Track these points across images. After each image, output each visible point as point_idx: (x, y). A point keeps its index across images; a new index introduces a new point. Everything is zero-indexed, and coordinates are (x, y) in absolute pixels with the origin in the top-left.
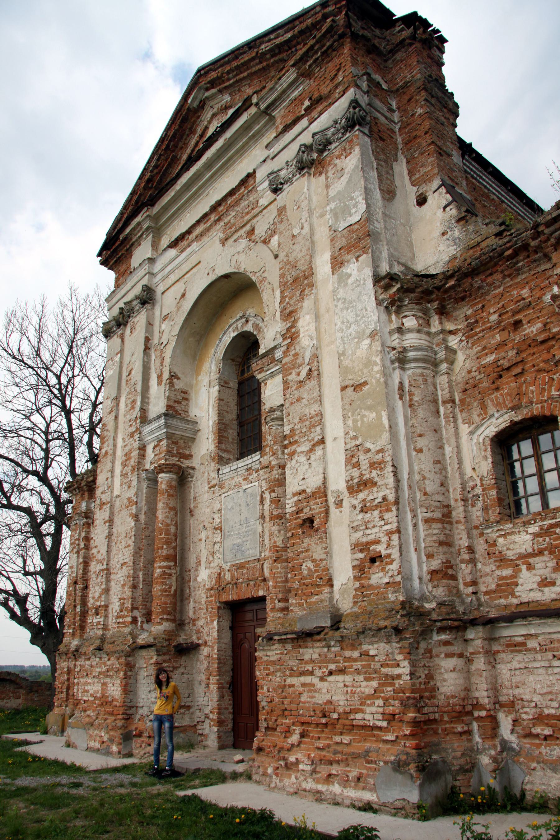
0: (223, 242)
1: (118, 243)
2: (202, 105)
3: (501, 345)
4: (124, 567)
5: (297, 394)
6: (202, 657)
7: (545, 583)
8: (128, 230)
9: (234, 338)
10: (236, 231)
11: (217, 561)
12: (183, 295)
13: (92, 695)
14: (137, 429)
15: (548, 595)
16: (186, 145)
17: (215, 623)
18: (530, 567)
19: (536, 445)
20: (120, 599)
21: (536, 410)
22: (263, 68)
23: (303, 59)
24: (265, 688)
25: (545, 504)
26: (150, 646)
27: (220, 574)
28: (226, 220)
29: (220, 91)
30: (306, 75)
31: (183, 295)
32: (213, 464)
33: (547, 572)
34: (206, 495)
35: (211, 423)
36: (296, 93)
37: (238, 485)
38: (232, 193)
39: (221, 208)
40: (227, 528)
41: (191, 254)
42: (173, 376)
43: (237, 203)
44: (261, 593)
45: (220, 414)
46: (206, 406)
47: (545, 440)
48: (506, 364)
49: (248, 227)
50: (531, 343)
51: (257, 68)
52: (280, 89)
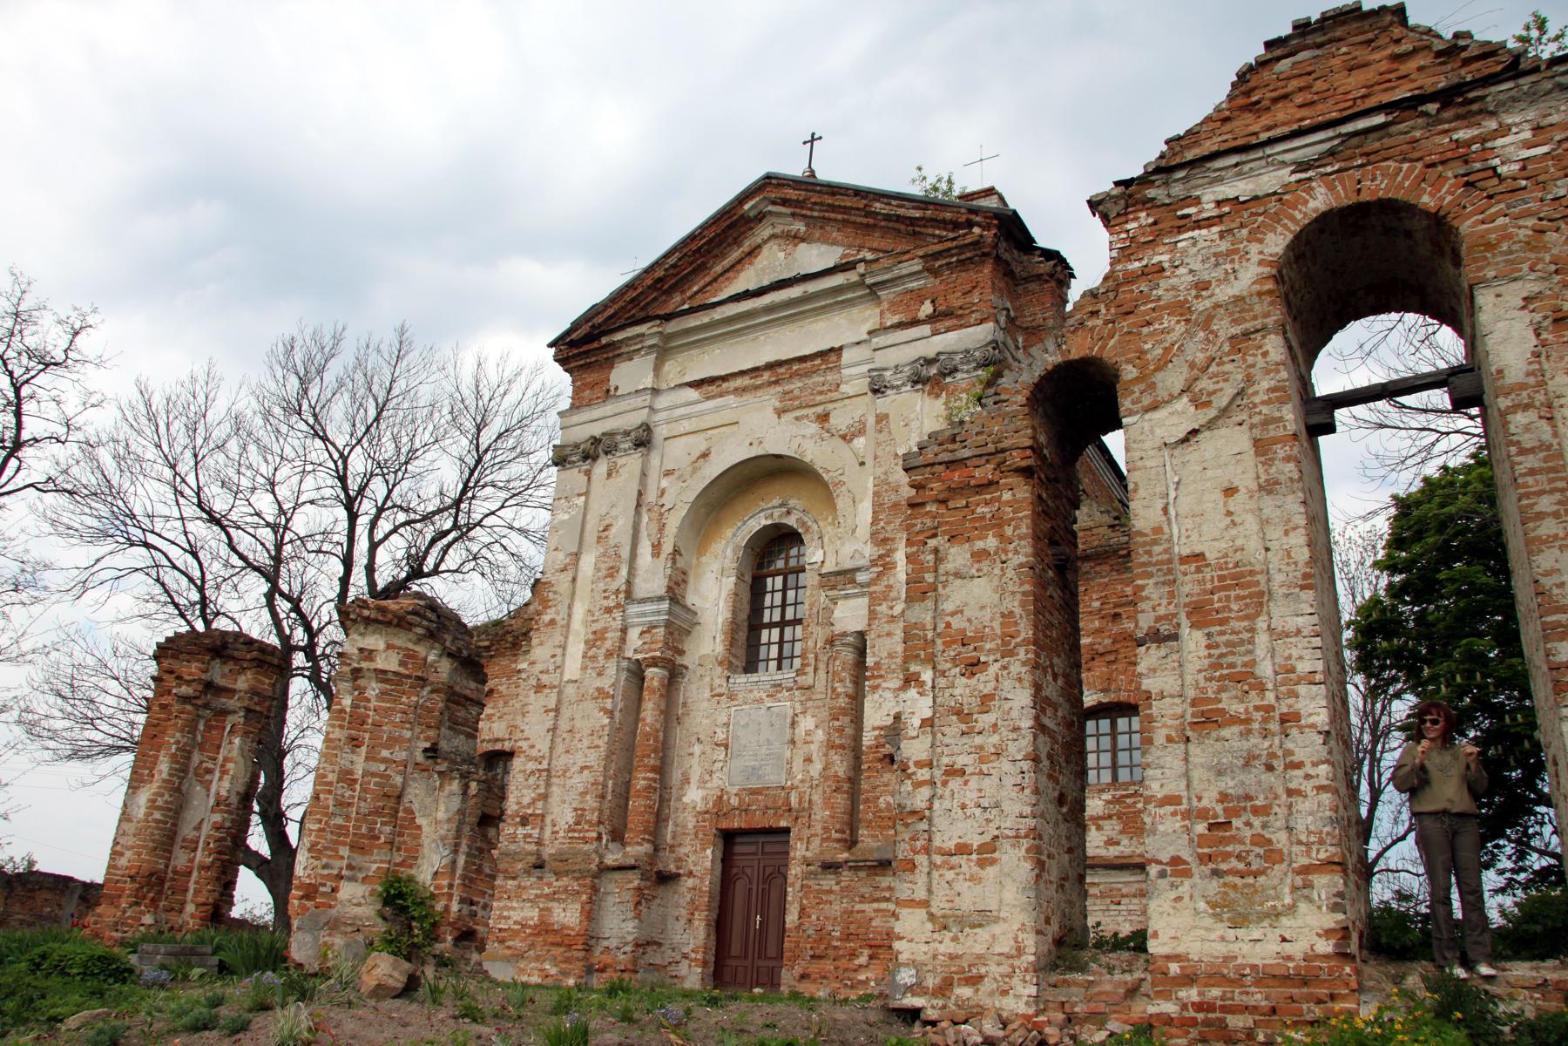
0: (780, 412)
1: (595, 345)
2: (760, 217)
3: (1099, 631)
4: (586, 772)
5: (887, 628)
6: (684, 889)
7: (1111, 842)
8: (619, 336)
9: (765, 527)
10: (801, 407)
11: (716, 782)
13: (516, 923)
14: (618, 606)
15: (1113, 851)
16: (723, 256)
17: (709, 852)
18: (1099, 828)
19: (1114, 725)
20: (576, 810)
21: (1123, 696)
22: (868, 225)
24: (814, 917)
25: (1115, 777)
26: (633, 868)
27: (720, 797)
28: (787, 388)
29: (793, 215)
30: (935, 273)
31: (705, 455)
32: (719, 669)
33: (1113, 834)
34: (705, 704)
35: (720, 620)
36: (915, 284)
37: (760, 701)
38: (802, 359)
39: (782, 370)
40: (734, 746)
41: (723, 408)
42: (676, 552)
43: (808, 374)
44: (783, 824)
45: (734, 613)
46: (715, 594)
47: (1122, 723)
48: (1101, 650)
49: (819, 409)
51: (859, 220)
52: (896, 273)
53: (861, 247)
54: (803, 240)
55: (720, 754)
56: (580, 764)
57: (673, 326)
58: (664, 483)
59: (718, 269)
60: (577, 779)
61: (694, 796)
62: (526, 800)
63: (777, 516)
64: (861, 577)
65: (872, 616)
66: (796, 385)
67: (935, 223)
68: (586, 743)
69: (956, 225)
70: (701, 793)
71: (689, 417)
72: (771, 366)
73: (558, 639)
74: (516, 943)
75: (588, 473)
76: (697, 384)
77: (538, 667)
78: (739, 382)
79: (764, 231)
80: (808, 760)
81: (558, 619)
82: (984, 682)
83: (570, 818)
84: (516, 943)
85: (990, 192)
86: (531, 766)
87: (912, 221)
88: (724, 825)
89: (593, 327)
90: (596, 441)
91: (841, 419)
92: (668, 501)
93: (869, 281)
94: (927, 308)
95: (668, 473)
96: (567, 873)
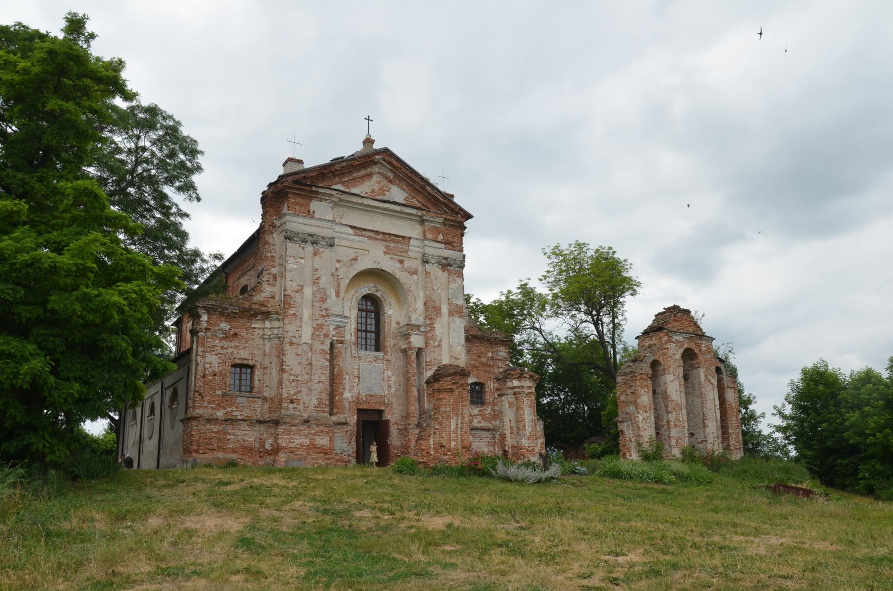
0: (386, 253)
1: (308, 188)
2: (376, 163)
11: (355, 391)
12: (355, 259)
15: (480, 425)
21: (482, 381)
23: (449, 220)
30: (444, 224)
31: (355, 259)
38: (396, 236)
43: (397, 242)
50: (482, 363)
53: (414, 197)
55: (356, 380)
57: (345, 197)
58: (337, 265)
59: (356, 175)
60: (316, 386)
61: (347, 395)
62: (292, 393)
63: (373, 291)
64: (422, 329)
65: (426, 343)
66: (392, 245)
67: (447, 206)
68: (319, 371)
69: (452, 210)
71: (348, 240)
72: (383, 233)
73: (298, 324)
75: (303, 248)
76: (353, 227)
77: (290, 334)
78: (370, 234)
79: (376, 169)
80: (390, 386)
81: (298, 314)
82: (648, 414)
83: (315, 402)
85: (452, 196)
86: (292, 378)
88: (361, 407)
89: (304, 177)
92: (341, 273)
93: (425, 218)
94: (441, 237)
95: (338, 261)
96: (322, 425)
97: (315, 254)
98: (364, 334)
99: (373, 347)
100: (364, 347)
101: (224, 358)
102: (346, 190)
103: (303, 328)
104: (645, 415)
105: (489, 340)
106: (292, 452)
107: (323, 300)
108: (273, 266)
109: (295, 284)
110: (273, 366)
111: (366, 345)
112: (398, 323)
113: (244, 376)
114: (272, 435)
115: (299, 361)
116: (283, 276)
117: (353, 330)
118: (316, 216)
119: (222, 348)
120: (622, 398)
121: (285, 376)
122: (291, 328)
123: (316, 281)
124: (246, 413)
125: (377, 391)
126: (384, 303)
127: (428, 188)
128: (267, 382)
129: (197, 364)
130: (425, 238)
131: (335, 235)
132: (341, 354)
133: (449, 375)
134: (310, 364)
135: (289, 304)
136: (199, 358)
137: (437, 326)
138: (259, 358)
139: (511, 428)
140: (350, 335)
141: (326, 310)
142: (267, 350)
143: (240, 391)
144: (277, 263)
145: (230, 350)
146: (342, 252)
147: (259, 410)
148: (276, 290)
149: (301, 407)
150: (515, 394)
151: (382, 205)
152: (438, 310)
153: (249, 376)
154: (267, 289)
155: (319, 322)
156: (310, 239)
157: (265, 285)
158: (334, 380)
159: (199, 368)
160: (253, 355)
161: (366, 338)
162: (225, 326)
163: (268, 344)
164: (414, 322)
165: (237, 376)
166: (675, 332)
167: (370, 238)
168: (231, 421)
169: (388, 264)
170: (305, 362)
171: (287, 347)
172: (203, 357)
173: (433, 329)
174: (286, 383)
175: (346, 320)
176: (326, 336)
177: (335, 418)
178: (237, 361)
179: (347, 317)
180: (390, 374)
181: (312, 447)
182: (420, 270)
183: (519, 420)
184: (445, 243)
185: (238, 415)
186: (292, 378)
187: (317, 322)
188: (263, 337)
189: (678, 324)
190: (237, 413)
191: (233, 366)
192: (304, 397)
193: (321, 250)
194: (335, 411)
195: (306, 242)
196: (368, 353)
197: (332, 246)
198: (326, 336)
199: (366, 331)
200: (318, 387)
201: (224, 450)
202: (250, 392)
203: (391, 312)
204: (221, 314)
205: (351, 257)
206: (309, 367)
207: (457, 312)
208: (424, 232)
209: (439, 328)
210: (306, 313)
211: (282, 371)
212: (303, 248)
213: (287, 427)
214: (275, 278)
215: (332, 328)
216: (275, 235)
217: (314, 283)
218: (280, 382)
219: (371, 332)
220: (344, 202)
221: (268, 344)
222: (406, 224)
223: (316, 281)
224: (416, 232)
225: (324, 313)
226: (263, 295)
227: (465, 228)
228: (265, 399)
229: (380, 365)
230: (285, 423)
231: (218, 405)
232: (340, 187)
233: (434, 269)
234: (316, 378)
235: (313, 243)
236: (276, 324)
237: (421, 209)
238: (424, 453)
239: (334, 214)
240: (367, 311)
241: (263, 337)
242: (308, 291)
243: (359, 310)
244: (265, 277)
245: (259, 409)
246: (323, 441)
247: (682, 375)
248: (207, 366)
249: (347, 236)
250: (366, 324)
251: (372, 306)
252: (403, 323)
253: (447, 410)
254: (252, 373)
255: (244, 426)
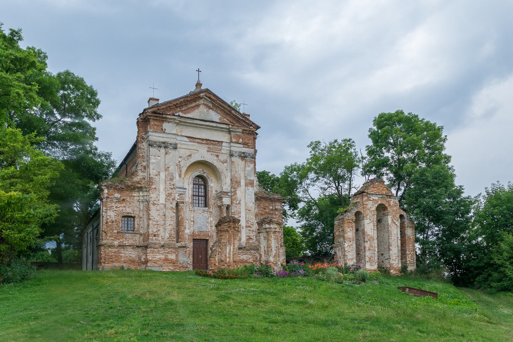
0: (208, 151)
30: (243, 133)
31: (190, 156)
35: (190, 194)
38: (214, 141)
43: (215, 145)
50: (266, 213)
53: (225, 118)
54: (211, 108)
56: (169, 224)
58: (180, 159)
60: (168, 227)
61: (187, 231)
62: (155, 231)
63: (201, 173)
64: (229, 194)
65: (232, 202)
66: (212, 146)
67: (244, 122)
68: (170, 219)
69: (248, 124)
70: (189, 231)
72: (206, 140)
74: (159, 263)
75: (159, 151)
77: (153, 199)
78: (198, 140)
80: (212, 226)
84: (159, 263)
85: (249, 115)
86: (154, 223)
87: (239, 119)
88: (195, 238)
90: (164, 143)
91: (222, 157)
94: (241, 141)
95: (180, 157)
97: (166, 154)
98: (197, 197)
99: (203, 205)
100: (197, 205)
101: (118, 213)
102: (185, 116)
103: (160, 195)
104: (350, 243)
105: (270, 199)
106: (155, 263)
107: (172, 179)
108: (143, 161)
109: (155, 171)
110: (145, 216)
111: (199, 203)
112: (216, 191)
113: (129, 222)
114: (145, 253)
115: (158, 214)
116: (148, 166)
117: (190, 195)
118: (166, 131)
119: (116, 207)
120: (337, 233)
121: (151, 222)
122: (153, 196)
123: (167, 169)
124: (131, 242)
125: (204, 229)
126: (208, 180)
127: (233, 112)
128: (142, 225)
129: (103, 216)
130: (231, 142)
131: (177, 142)
132: (183, 209)
133: (226, 222)
134: (165, 215)
135: (152, 182)
136: (104, 213)
137: (238, 192)
138: (137, 212)
139: (265, 251)
140: (188, 197)
141: (173, 185)
142: (142, 208)
143: (128, 230)
144: (145, 160)
145: (121, 208)
146: (182, 152)
147: (138, 240)
148: (145, 174)
149: (160, 238)
150: (267, 232)
151: (205, 124)
152: (238, 183)
153: (132, 222)
154: (141, 175)
155: (169, 192)
156: (163, 145)
157: (139, 172)
158: (179, 223)
159: (104, 219)
160: (134, 211)
161: (199, 200)
162: (117, 195)
163: (142, 205)
164: (225, 190)
165: (126, 222)
166: (372, 194)
167: (197, 142)
168: (122, 246)
169: (209, 158)
170: (162, 214)
171: (151, 206)
172: (106, 212)
173: (236, 194)
174: (151, 226)
175: (185, 190)
176: (173, 199)
177: (179, 244)
178: (125, 214)
179: (185, 189)
180: (212, 219)
181: (166, 260)
182: (228, 161)
183: (269, 247)
184: (243, 144)
185: (126, 243)
186: (154, 223)
187: (168, 192)
188: (138, 201)
189: (375, 189)
190: (126, 242)
191: (123, 217)
192: (161, 233)
193: (170, 151)
194: (179, 240)
195: (161, 147)
196: (199, 208)
197: (175, 148)
198: (173, 199)
199: (199, 196)
200: (169, 228)
201: (119, 262)
202: (133, 231)
203: (212, 185)
204: (115, 189)
205: (187, 155)
206: (164, 217)
207: (250, 184)
208: (231, 138)
209: (240, 193)
210: (162, 187)
211: (149, 219)
212: (159, 151)
213: (152, 249)
214: (145, 168)
215: (177, 195)
216: (144, 144)
217: (166, 170)
218: (148, 225)
219: (201, 196)
220: (183, 122)
221: (142, 205)
222: (220, 133)
223: (167, 169)
224: (226, 138)
225: (172, 187)
226: (139, 177)
227: (257, 134)
228: (141, 234)
229: (206, 215)
230: (151, 247)
231: (115, 238)
232: (181, 114)
233: (237, 160)
234: (168, 223)
235: (165, 147)
236: (146, 194)
237: (229, 125)
238: (212, 265)
239: (177, 130)
240: (199, 185)
241: (138, 201)
242: (163, 175)
243: (194, 184)
244: (139, 168)
245: (138, 240)
246: (172, 257)
247: (375, 220)
248: (108, 217)
249: (185, 143)
250: (199, 192)
251: (201, 181)
252: (219, 191)
253: (225, 241)
254: (134, 220)
255: (130, 249)
